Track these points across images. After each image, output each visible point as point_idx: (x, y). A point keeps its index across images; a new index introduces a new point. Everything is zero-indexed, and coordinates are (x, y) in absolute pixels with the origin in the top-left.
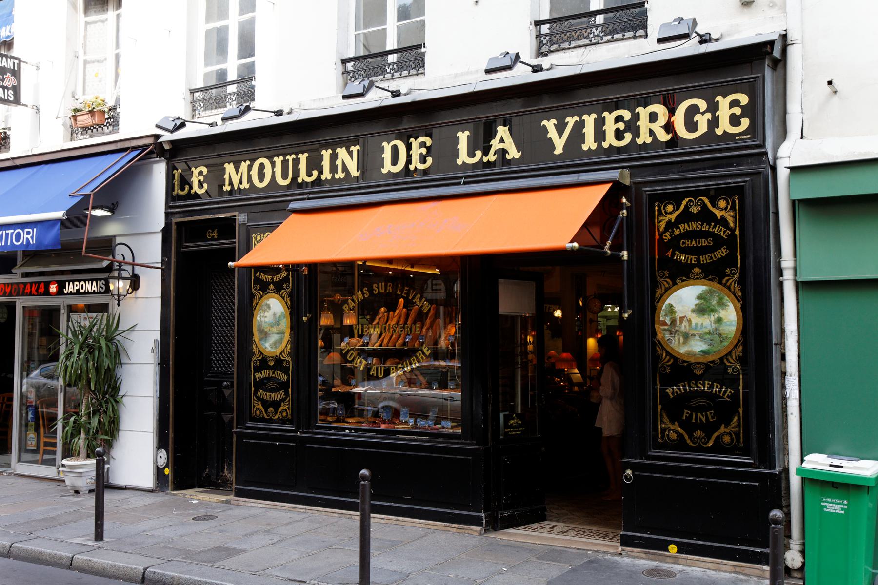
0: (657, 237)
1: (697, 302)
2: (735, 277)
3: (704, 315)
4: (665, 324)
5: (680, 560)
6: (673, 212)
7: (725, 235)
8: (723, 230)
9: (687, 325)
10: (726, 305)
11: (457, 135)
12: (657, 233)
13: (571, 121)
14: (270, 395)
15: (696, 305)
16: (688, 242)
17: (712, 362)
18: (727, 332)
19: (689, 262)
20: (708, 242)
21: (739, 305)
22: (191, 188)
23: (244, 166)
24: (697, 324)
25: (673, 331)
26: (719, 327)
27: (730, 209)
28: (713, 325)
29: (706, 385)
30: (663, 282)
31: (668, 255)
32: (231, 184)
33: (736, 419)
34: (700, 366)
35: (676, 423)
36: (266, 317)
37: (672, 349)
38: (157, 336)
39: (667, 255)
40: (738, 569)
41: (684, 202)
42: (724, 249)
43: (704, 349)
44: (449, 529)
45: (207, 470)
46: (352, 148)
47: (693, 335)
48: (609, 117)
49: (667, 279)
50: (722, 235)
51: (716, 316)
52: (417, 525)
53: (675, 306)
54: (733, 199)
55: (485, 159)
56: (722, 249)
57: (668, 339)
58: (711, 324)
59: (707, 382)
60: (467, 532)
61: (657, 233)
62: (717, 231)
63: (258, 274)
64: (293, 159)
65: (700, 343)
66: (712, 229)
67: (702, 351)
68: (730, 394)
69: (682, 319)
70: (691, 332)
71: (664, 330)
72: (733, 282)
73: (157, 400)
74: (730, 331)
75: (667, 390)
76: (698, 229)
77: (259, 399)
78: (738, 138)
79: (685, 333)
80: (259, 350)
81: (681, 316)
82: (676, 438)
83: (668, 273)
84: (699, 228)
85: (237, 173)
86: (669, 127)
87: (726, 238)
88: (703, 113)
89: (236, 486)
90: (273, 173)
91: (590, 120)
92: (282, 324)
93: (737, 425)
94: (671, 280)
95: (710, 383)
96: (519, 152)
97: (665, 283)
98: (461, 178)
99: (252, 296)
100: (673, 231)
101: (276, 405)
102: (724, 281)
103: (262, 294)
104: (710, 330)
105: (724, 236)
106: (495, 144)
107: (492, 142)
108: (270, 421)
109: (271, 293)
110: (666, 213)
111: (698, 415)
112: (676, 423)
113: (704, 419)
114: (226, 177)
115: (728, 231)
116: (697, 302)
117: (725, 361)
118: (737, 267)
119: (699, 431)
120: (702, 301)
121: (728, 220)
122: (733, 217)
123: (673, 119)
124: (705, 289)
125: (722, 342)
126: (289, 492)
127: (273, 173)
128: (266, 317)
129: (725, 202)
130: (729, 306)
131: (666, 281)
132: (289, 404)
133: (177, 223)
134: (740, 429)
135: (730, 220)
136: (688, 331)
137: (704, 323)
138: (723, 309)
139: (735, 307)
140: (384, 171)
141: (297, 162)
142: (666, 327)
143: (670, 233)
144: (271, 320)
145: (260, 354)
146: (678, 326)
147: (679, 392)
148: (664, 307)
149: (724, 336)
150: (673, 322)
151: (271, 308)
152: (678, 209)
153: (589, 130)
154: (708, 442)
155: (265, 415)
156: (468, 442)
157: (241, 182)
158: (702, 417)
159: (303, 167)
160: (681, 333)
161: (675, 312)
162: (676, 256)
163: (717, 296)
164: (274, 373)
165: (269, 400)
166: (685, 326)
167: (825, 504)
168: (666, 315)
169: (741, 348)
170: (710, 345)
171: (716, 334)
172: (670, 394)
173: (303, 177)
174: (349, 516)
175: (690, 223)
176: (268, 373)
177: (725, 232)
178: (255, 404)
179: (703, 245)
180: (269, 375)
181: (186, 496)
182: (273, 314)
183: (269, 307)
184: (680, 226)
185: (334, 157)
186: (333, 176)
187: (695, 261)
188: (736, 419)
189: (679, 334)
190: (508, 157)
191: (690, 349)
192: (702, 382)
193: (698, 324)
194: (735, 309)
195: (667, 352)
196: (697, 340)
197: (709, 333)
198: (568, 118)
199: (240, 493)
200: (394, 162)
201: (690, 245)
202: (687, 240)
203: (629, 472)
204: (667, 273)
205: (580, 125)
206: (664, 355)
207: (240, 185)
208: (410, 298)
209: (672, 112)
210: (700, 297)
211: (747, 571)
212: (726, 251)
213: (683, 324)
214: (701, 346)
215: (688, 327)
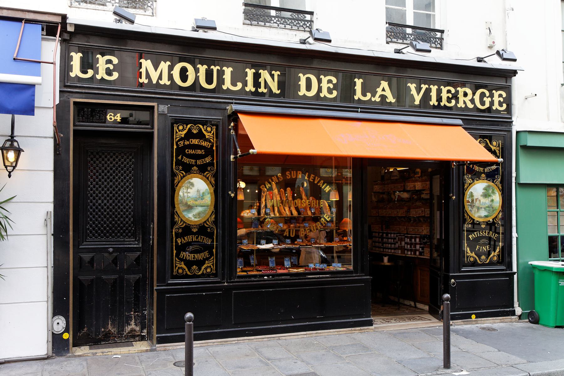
1: (483, 191)
3: (486, 198)
4: (468, 202)
5: (479, 321)
9: (479, 202)
10: (495, 193)
11: (441, 88)
13: (424, 87)
14: (194, 256)
15: (483, 193)
18: (496, 206)
19: (480, 171)
21: (500, 193)
22: (96, 72)
23: (164, 66)
24: (483, 202)
27: (498, 146)
28: (490, 203)
29: (487, 233)
32: (148, 76)
36: (189, 193)
38: (50, 208)
40: (502, 321)
44: (354, 331)
45: (86, 329)
46: (273, 72)
47: (481, 208)
48: (444, 90)
51: (491, 198)
52: (331, 334)
55: (373, 99)
60: (366, 331)
63: (180, 158)
64: (218, 70)
65: (484, 212)
69: (476, 199)
70: (481, 206)
71: (468, 205)
73: (51, 270)
75: (469, 236)
77: (181, 260)
78: (502, 113)
80: (181, 219)
81: (476, 198)
83: (182, 167)
85: (156, 70)
86: (472, 101)
88: (487, 97)
89: (157, 335)
90: (197, 78)
91: (434, 88)
92: (206, 198)
93: (499, 251)
94: (184, 172)
96: (394, 99)
97: (469, 181)
98: (358, 108)
99: (174, 175)
101: (200, 263)
102: (494, 182)
103: (185, 174)
106: (379, 91)
107: (378, 90)
108: (198, 277)
109: (195, 173)
114: (143, 70)
116: (483, 191)
117: (495, 220)
118: (500, 175)
119: (195, 266)
120: (485, 191)
122: (499, 151)
123: (474, 97)
125: (493, 211)
126: (216, 331)
127: (197, 78)
128: (189, 193)
130: (496, 193)
131: (470, 180)
132: (213, 261)
133: (75, 103)
134: (500, 253)
135: (497, 152)
139: (499, 194)
140: (301, 94)
141: (221, 73)
142: (469, 204)
144: (195, 195)
145: (182, 222)
147: (475, 237)
148: (468, 194)
150: (473, 201)
151: (195, 186)
153: (434, 94)
155: (189, 273)
156: (358, 274)
157: (160, 78)
158: (484, 248)
159: (227, 76)
162: (183, 159)
163: (492, 189)
164: (197, 238)
165: (192, 259)
167: (560, 282)
168: (469, 197)
170: (488, 213)
172: (471, 237)
173: (228, 85)
174: (277, 338)
176: (191, 238)
178: (177, 264)
180: (192, 239)
181: (97, 354)
182: (197, 190)
183: (192, 184)
185: (257, 76)
186: (257, 90)
187: (482, 171)
190: (388, 101)
191: (480, 215)
194: (499, 195)
195: (470, 216)
197: (488, 207)
198: (300, 74)
199: (161, 341)
200: (309, 88)
202: (190, 150)
203: (453, 280)
204: (470, 176)
205: (428, 91)
206: (468, 218)
207: (160, 81)
208: (316, 182)
209: (474, 94)
210: (484, 189)
211: (506, 320)
214: (485, 213)
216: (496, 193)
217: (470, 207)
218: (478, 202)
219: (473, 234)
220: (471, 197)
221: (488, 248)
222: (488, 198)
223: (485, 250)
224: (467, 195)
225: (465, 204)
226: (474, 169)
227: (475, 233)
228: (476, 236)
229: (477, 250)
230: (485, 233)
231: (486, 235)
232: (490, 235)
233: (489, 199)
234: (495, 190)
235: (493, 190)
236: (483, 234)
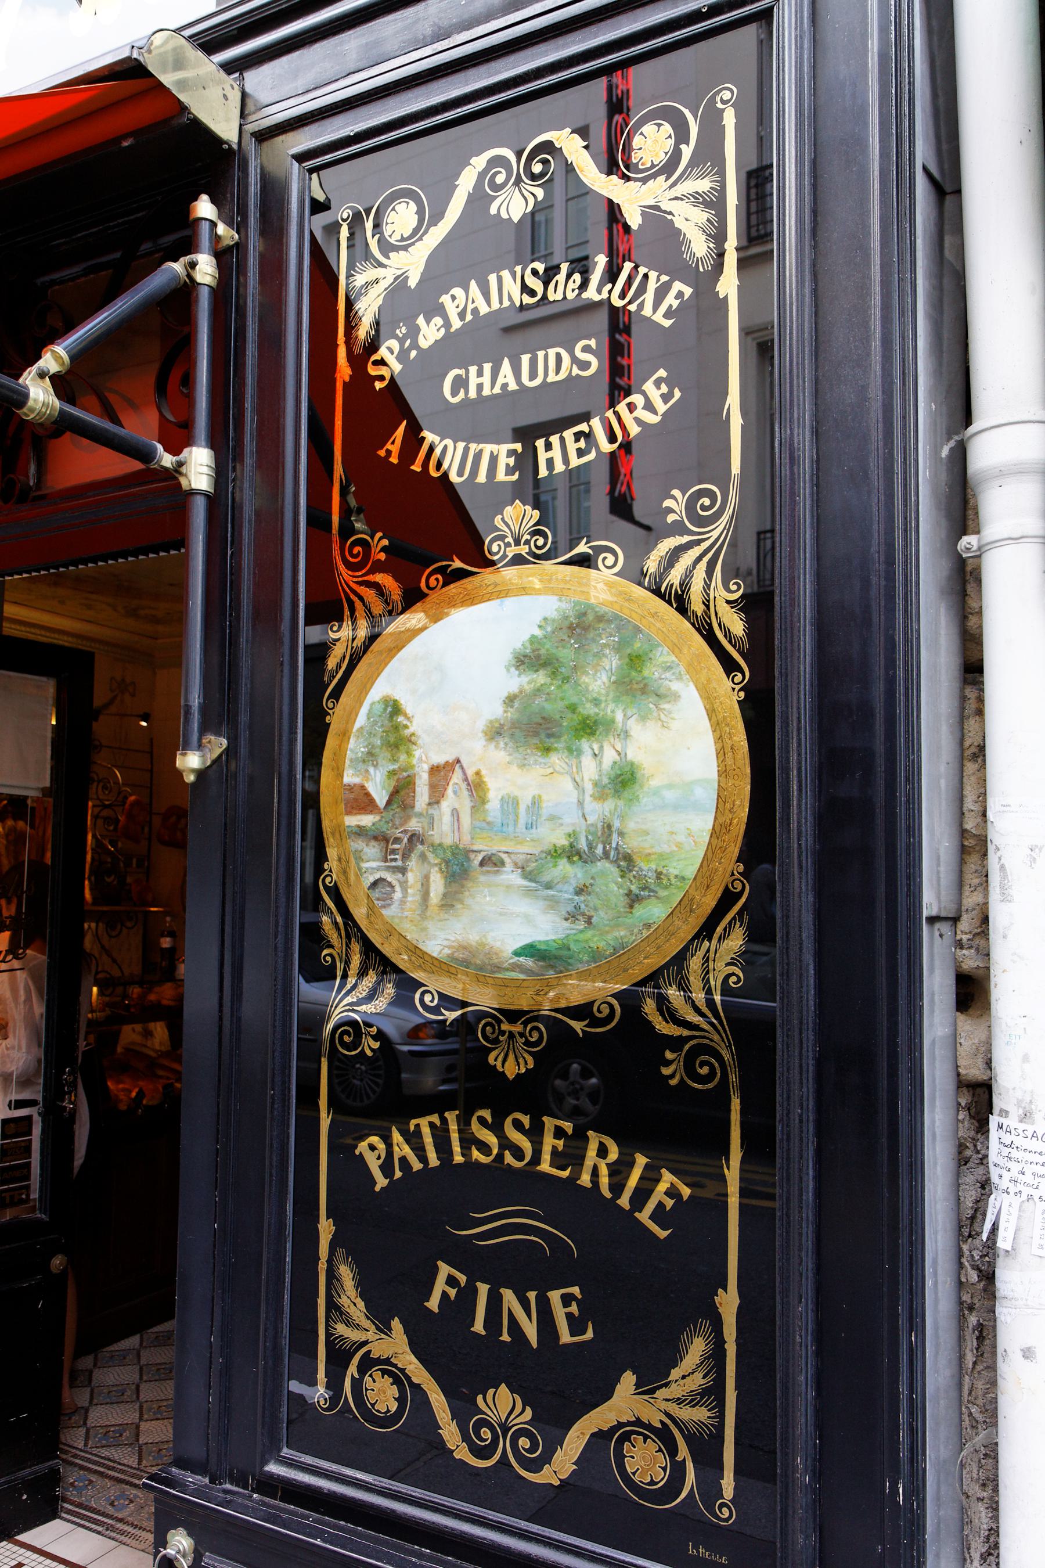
0: (344, 369)
2: (715, 534)
3: (548, 750)
4: (362, 802)
6: (418, 233)
7: (663, 308)
8: (649, 296)
9: (465, 805)
12: (342, 352)
15: (510, 700)
16: (480, 374)
17: (582, 1011)
18: (665, 848)
19: (482, 478)
20: (575, 360)
24: (510, 803)
25: (397, 840)
26: (622, 817)
27: (692, 164)
29: (549, 1142)
30: (362, 590)
31: (389, 453)
33: (697, 1348)
34: (518, 1028)
35: (396, 1324)
37: (391, 931)
39: (382, 453)
41: (466, 181)
42: (658, 383)
43: (542, 937)
47: (493, 862)
49: (379, 578)
50: (647, 311)
51: (609, 756)
53: (409, 711)
54: (712, 101)
56: (649, 386)
57: (375, 884)
58: (581, 803)
59: (549, 1122)
61: (342, 352)
62: (623, 295)
66: (599, 291)
67: (530, 950)
68: (669, 1203)
69: (440, 773)
70: (484, 846)
71: (361, 832)
72: (703, 565)
74: (681, 838)
75: (363, 1147)
76: (527, 300)
79: (455, 849)
81: (439, 759)
82: (394, 1407)
84: (532, 293)
87: (667, 323)
93: (705, 1392)
95: (568, 1126)
100: (414, 332)
102: (652, 565)
104: (573, 835)
105: (659, 317)
110: (386, 248)
111: (501, 1296)
112: (396, 1324)
113: (531, 1330)
115: (678, 286)
117: (649, 1007)
118: (723, 479)
120: (541, 677)
121: (679, 223)
122: (707, 204)
124: (553, 614)
125: (633, 900)
129: (667, 128)
130: (676, 697)
134: (721, 1416)
136: (466, 838)
137: (544, 797)
138: (643, 718)
142: (367, 820)
143: (401, 341)
146: (420, 815)
147: (417, 1165)
148: (361, 720)
149: (647, 867)
152: (437, 217)
154: (547, 1458)
160: (436, 848)
161: (410, 740)
163: (618, 649)
166: (455, 813)
168: (371, 757)
169: (736, 941)
170: (571, 917)
171: (606, 855)
172: (374, 1165)
175: (493, 278)
177: (661, 293)
179: (552, 378)
184: (445, 299)
188: (697, 1348)
189: (423, 857)
191: (473, 938)
192: (526, 1120)
193: (516, 802)
194: (711, 712)
196: (509, 887)
197: (572, 853)
201: (486, 392)
212: (666, 398)
213: (446, 805)
214: (528, 919)
215: (466, 820)
216: (676, 697)
217: (371, 851)
218: (455, 798)
219: (397, 1137)
220: (384, 755)
221: (560, 1313)
222: (574, 752)
223: (531, 1330)
224: (345, 735)
225: (326, 824)
226: (417, 467)
227: (424, 1123)
228: (433, 1160)
229: (433, 1303)
230: (526, 1145)
231: (545, 1166)
232: (595, 1172)
233: (588, 764)
234: (663, 655)
235: (635, 661)
236: (505, 1144)
